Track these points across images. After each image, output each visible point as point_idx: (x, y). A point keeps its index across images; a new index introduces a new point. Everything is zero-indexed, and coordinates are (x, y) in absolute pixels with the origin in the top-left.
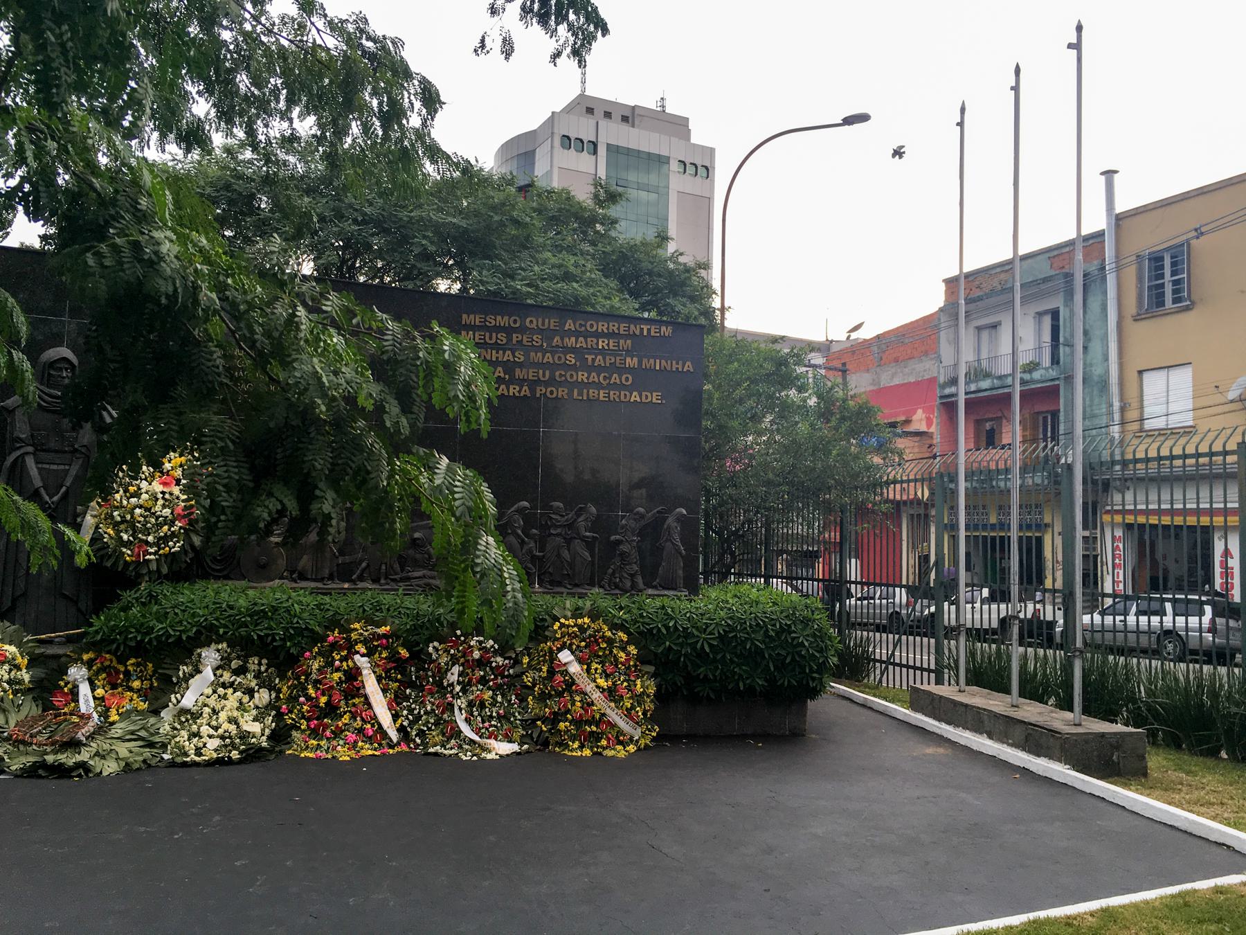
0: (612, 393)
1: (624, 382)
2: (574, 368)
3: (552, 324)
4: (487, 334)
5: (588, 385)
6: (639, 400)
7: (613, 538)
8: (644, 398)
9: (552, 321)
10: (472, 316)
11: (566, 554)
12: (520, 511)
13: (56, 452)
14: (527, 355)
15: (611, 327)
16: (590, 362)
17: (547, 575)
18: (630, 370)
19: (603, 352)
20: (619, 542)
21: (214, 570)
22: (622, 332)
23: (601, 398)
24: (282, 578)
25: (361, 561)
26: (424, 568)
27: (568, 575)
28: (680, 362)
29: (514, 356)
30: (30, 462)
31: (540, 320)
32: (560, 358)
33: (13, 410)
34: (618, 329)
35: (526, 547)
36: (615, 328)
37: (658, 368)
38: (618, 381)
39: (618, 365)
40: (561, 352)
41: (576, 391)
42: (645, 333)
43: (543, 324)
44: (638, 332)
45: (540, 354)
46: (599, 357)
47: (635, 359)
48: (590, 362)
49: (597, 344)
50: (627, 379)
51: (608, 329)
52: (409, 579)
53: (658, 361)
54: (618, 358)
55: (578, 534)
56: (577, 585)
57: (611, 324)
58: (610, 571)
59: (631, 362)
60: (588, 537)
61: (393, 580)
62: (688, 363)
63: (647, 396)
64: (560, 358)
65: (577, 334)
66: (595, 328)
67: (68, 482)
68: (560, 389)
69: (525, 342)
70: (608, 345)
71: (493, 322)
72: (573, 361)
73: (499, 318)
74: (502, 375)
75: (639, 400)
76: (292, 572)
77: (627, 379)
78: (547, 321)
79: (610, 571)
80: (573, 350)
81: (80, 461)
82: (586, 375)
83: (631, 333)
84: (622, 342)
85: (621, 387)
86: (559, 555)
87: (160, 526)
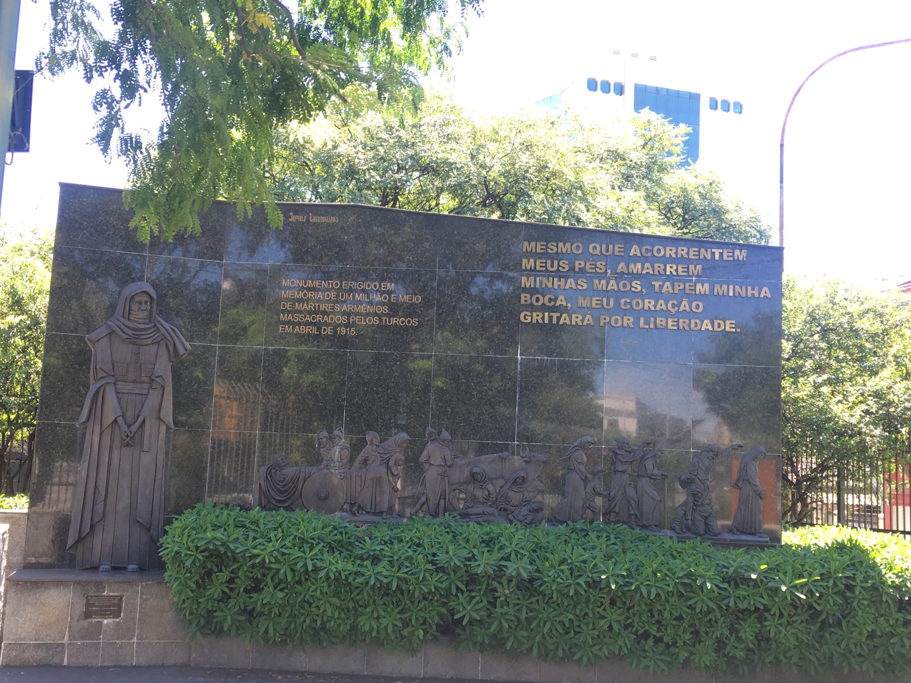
0: (681, 321)
1: (694, 310)
2: (640, 295)
3: (617, 250)
4: (549, 262)
5: (655, 313)
6: (710, 328)
8: (716, 326)
9: (616, 247)
10: (533, 244)
11: (631, 492)
13: (135, 382)
14: (590, 282)
15: (680, 252)
16: (657, 289)
17: (613, 515)
18: (702, 297)
19: (670, 277)
22: (691, 257)
23: (670, 327)
26: (483, 503)
28: (756, 288)
31: (604, 246)
32: (625, 285)
34: (688, 253)
37: (731, 294)
38: (687, 309)
39: (687, 291)
40: (626, 279)
41: (642, 321)
42: (717, 257)
43: (607, 251)
44: (709, 257)
45: (603, 282)
46: (667, 284)
47: (706, 286)
48: (657, 289)
49: (665, 270)
50: (698, 307)
51: (676, 253)
53: (731, 287)
54: (687, 285)
57: (680, 248)
59: (702, 288)
60: (656, 475)
62: (765, 289)
63: (719, 325)
64: (625, 285)
65: (643, 259)
66: (662, 253)
68: (625, 318)
69: (588, 269)
70: (677, 270)
71: (555, 249)
72: (639, 288)
73: (561, 244)
74: (564, 303)
75: (710, 328)
77: (698, 307)
78: (611, 247)
80: (638, 276)
82: (653, 302)
83: (702, 257)
84: (692, 267)
85: (690, 315)
86: (624, 493)
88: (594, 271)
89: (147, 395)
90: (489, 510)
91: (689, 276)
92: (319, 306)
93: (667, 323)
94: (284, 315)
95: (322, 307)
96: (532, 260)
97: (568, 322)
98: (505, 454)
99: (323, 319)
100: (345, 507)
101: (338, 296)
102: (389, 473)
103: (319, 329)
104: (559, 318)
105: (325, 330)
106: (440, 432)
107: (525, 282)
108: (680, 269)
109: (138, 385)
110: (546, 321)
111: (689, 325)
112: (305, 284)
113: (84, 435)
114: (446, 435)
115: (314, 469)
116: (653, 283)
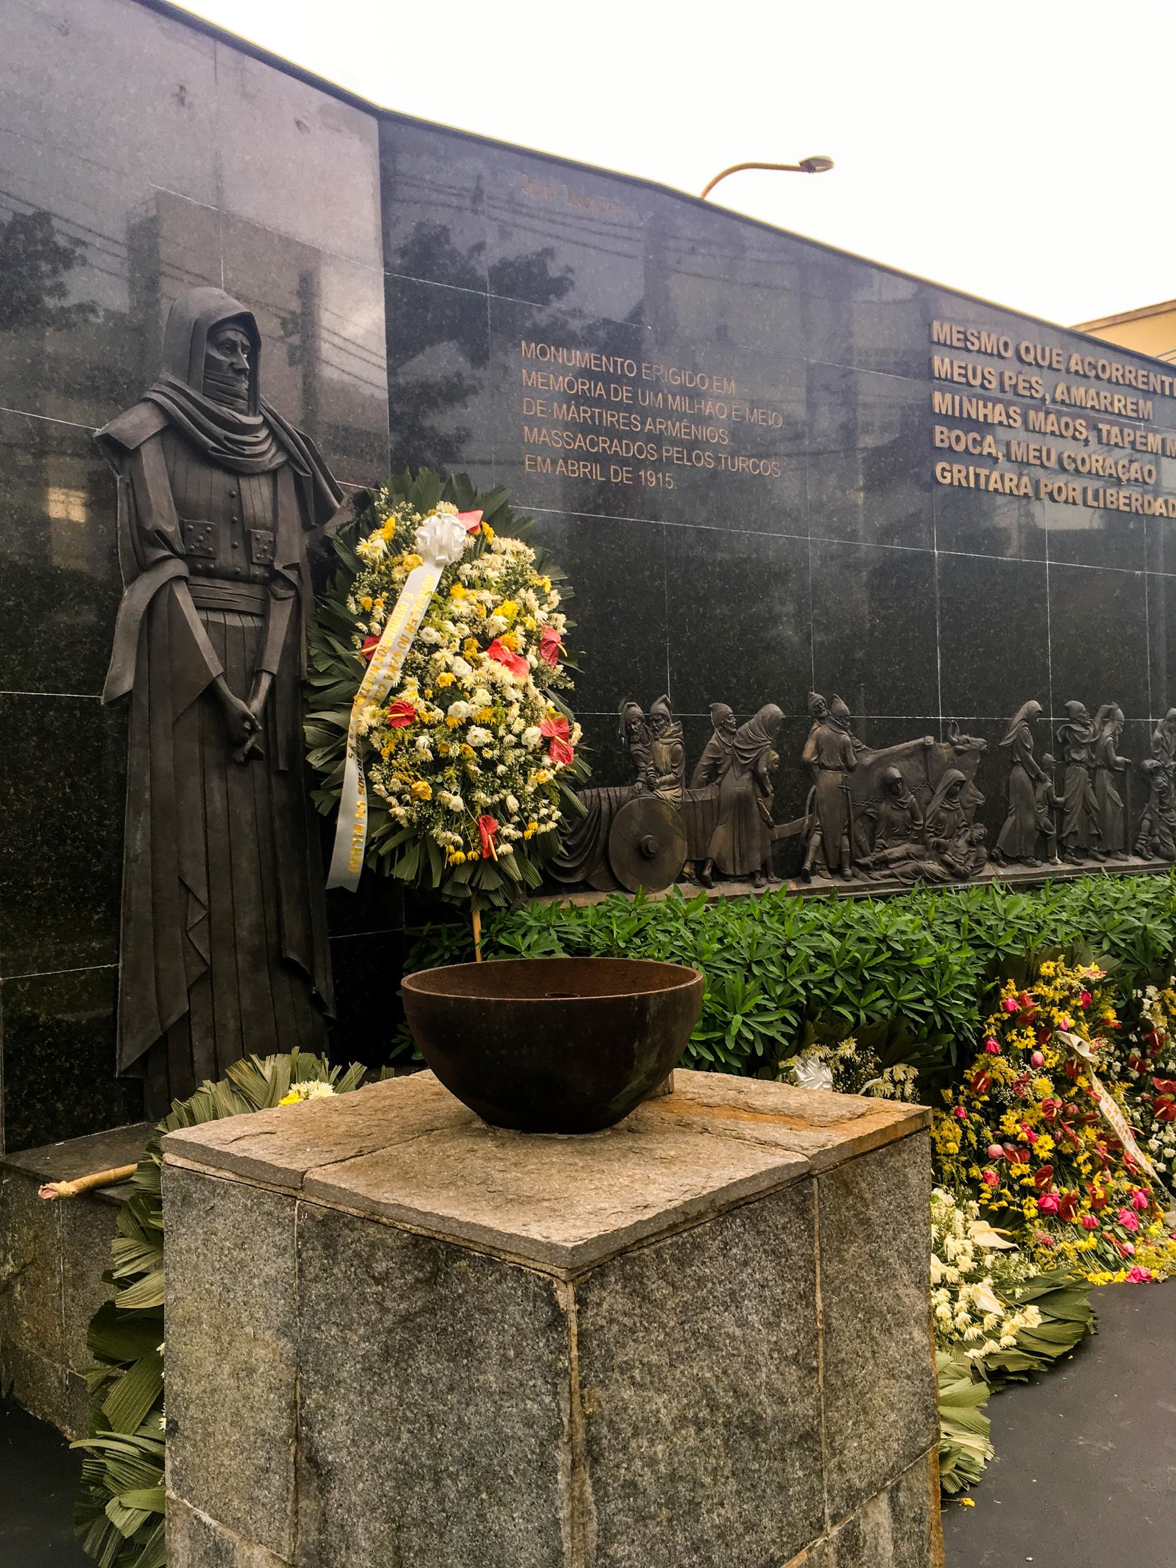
3: (1055, 358)
7: (1149, 763)
11: (1093, 799)
12: (1029, 719)
13: (234, 577)
15: (1127, 375)
20: (1155, 771)
21: (567, 872)
24: (681, 879)
25: (808, 837)
26: (903, 837)
27: (1099, 836)
29: (1009, 416)
30: (183, 597)
33: (138, 449)
35: (1041, 789)
36: (1132, 376)
45: (1042, 415)
52: (884, 863)
55: (1107, 758)
56: (1108, 854)
58: (1146, 823)
60: (1117, 764)
61: (865, 868)
67: (273, 661)
70: (1125, 407)
74: (993, 451)
76: (700, 865)
79: (1146, 823)
81: (288, 607)
87: (524, 769)
88: (1027, 393)
89: (264, 615)
90: (914, 848)
91: (1138, 419)
92: (600, 414)
93: (1118, 499)
94: (531, 431)
95: (608, 418)
96: (947, 360)
97: (999, 486)
98: (930, 739)
99: (610, 447)
100: (686, 870)
101: (634, 397)
102: (758, 790)
103: (605, 471)
104: (988, 477)
105: (616, 472)
106: (830, 702)
107: (942, 402)
108: (1130, 407)
109: (243, 589)
110: (972, 485)
111: (1142, 506)
112: (569, 360)
113: (124, 730)
114: (842, 705)
115: (624, 791)
116: (1100, 426)
